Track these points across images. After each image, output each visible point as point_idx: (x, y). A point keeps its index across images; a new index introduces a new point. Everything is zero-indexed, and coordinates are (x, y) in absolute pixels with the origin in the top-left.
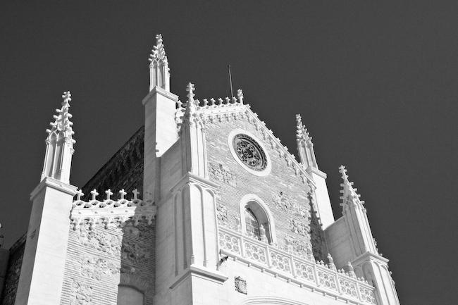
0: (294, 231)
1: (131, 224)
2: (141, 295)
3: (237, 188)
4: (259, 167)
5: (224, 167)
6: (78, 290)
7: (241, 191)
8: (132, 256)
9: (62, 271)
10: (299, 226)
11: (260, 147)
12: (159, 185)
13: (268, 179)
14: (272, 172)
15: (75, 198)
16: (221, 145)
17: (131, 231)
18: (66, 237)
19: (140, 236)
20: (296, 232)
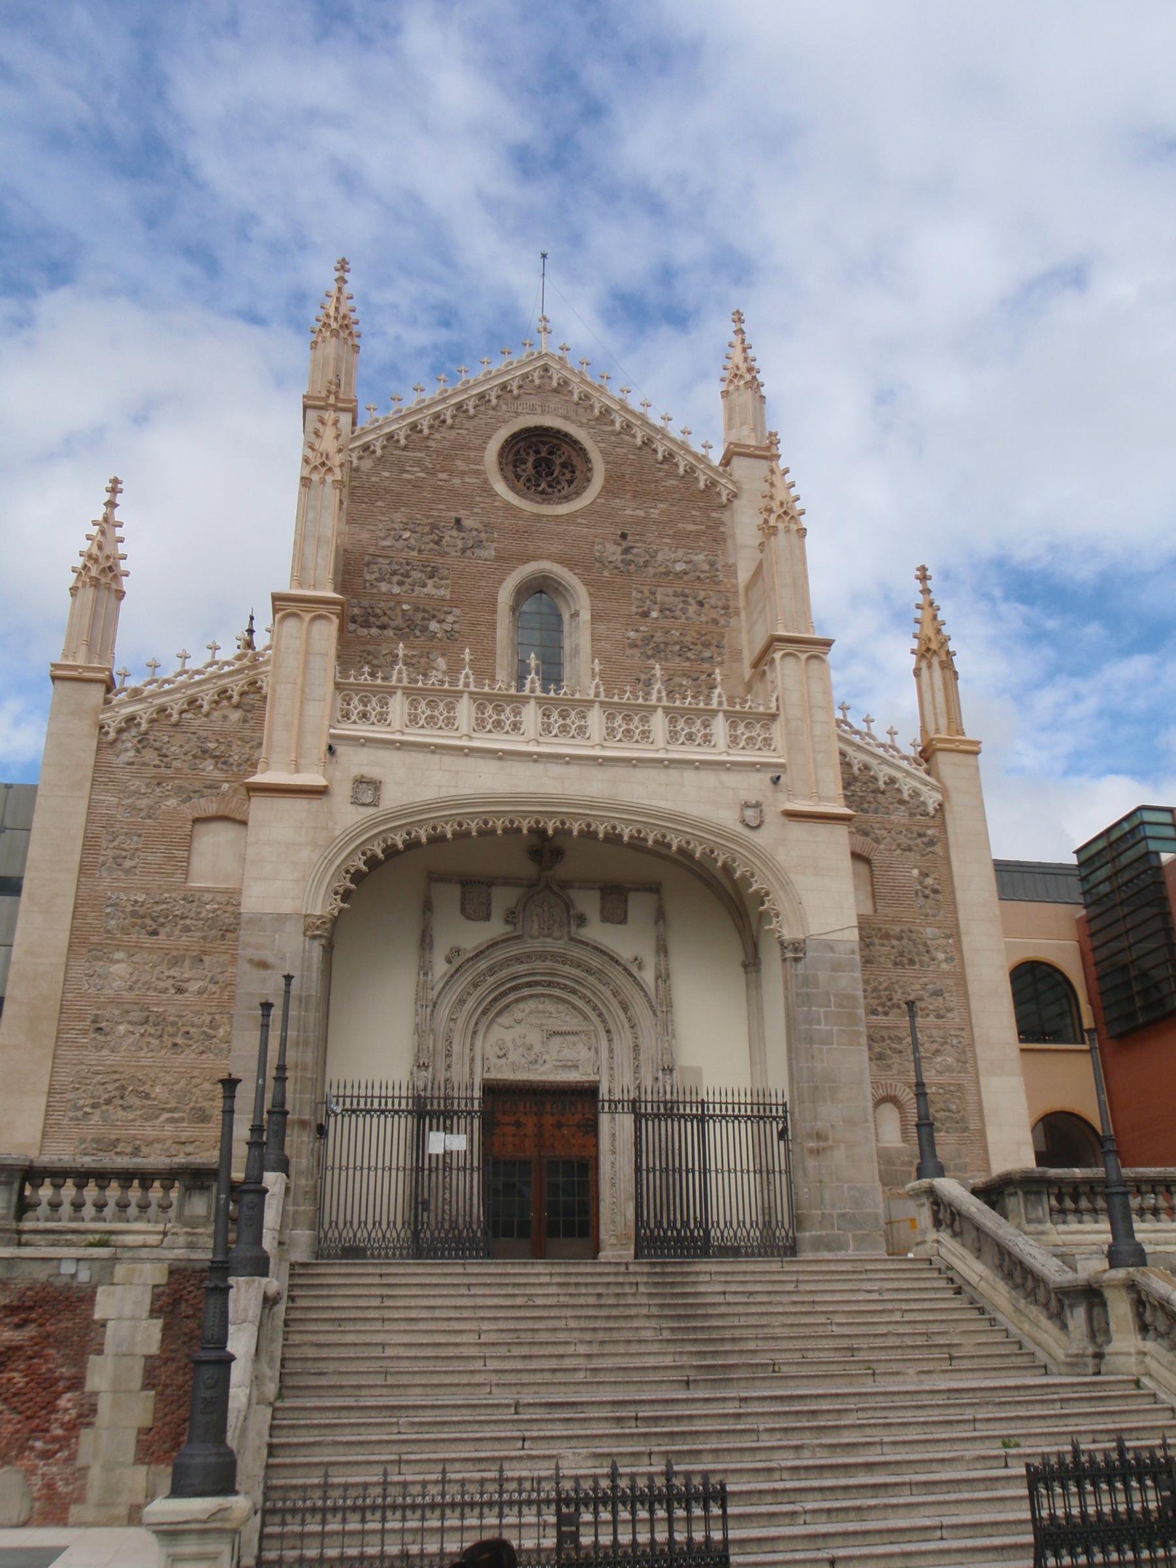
0: (645, 615)
1: (225, 703)
5: (467, 523)
6: (115, 843)
7: (507, 560)
8: (225, 763)
9: (80, 821)
11: (576, 442)
14: (606, 490)
16: (463, 473)
17: (225, 717)
18: (90, 759)
19: (245, 721)
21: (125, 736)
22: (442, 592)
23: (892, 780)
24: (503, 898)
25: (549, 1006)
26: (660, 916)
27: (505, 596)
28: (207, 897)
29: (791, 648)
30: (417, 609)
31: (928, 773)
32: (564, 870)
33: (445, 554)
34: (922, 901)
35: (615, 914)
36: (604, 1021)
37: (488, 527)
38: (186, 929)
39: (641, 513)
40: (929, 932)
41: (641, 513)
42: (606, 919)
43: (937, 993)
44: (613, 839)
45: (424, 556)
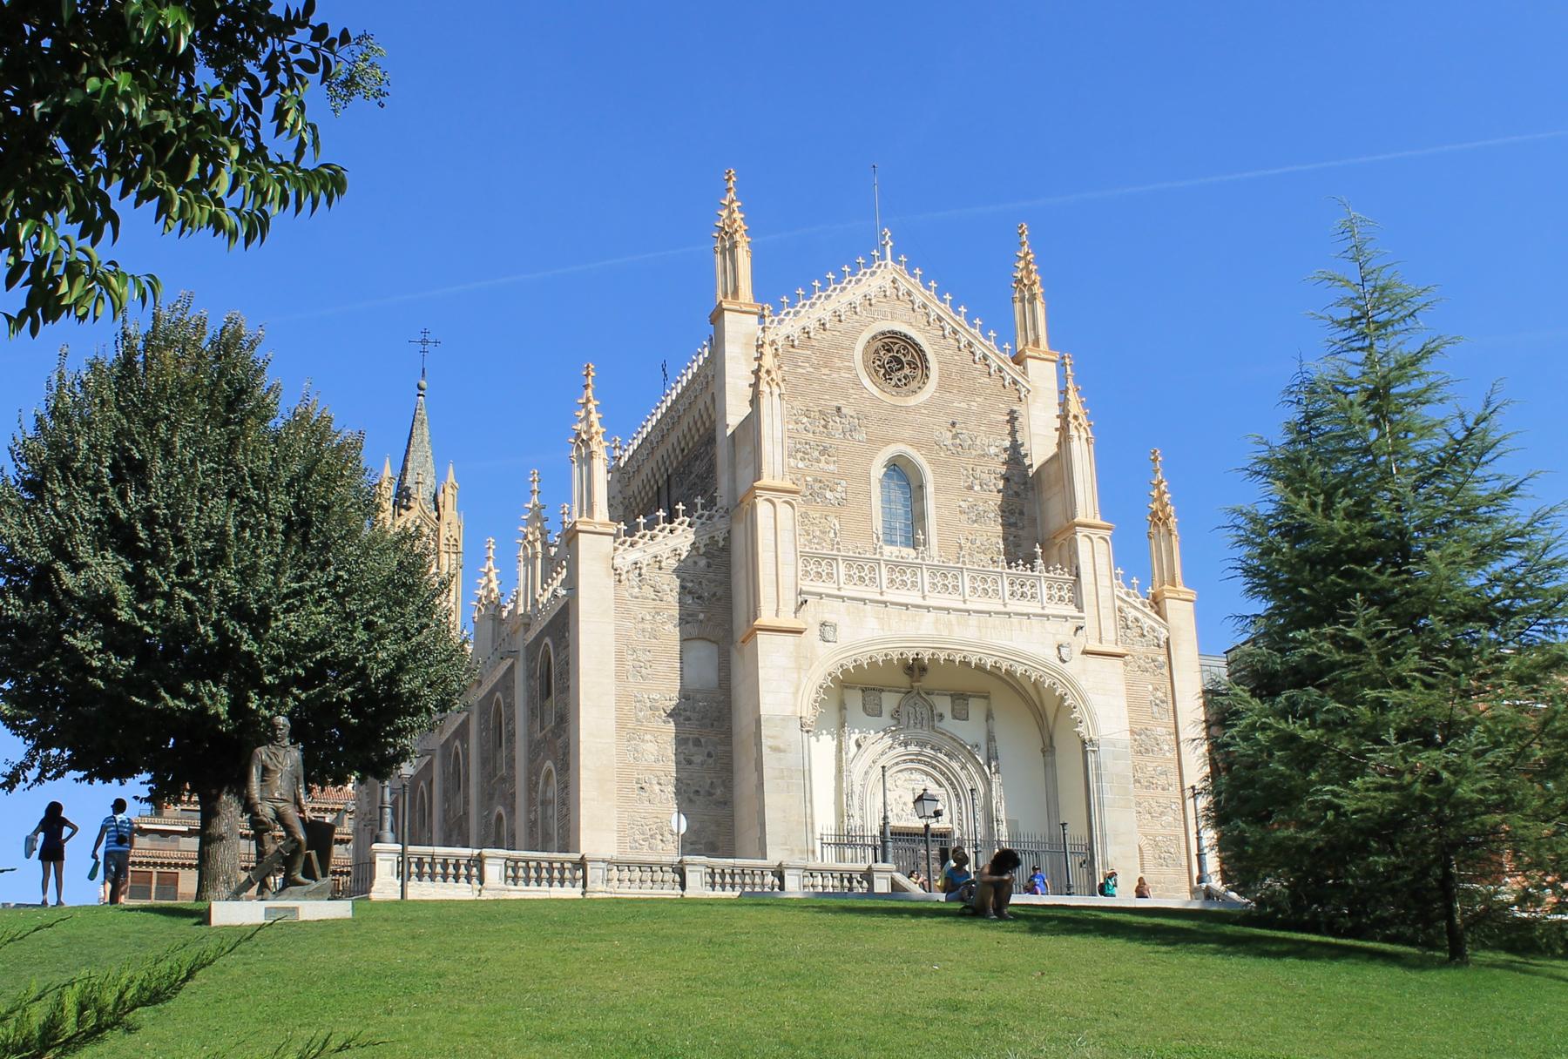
0: (971, 488)
2: (715, 647)
3: (869, 441)
4: (914, 385)
5: (844, 410)
10: (985, 476)
12: (733, 479)
13: (926, 405)
14: (940, 386)
15: (616, 536)
18: (611, 594)
20: (977, 488)
21: (631, 575)
22: (832, 467)
23: (1137, 620)
24: (890, 701)
25: (916, 776)
26: (989, 716)
27: (878, 470)
28: (698, 696)
29: (1087, 531)
30: (815, 480)
31: (1157, 613)
32: (928, 681)
33: (829, 435)
34: (1155, 709)
35: (961, 715)
36: (954, 788)
37: (862, 416)
38: (688, 719)
39: (963, 405)
40: (1160, 730)
41: (963, 405)
42: (955, 717)
43: (1164, 773)
44: (980, 668)
45: (818, 438)
